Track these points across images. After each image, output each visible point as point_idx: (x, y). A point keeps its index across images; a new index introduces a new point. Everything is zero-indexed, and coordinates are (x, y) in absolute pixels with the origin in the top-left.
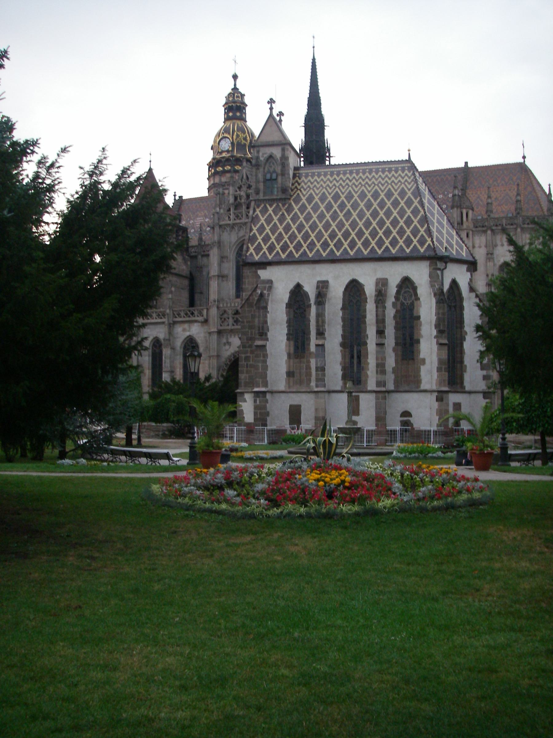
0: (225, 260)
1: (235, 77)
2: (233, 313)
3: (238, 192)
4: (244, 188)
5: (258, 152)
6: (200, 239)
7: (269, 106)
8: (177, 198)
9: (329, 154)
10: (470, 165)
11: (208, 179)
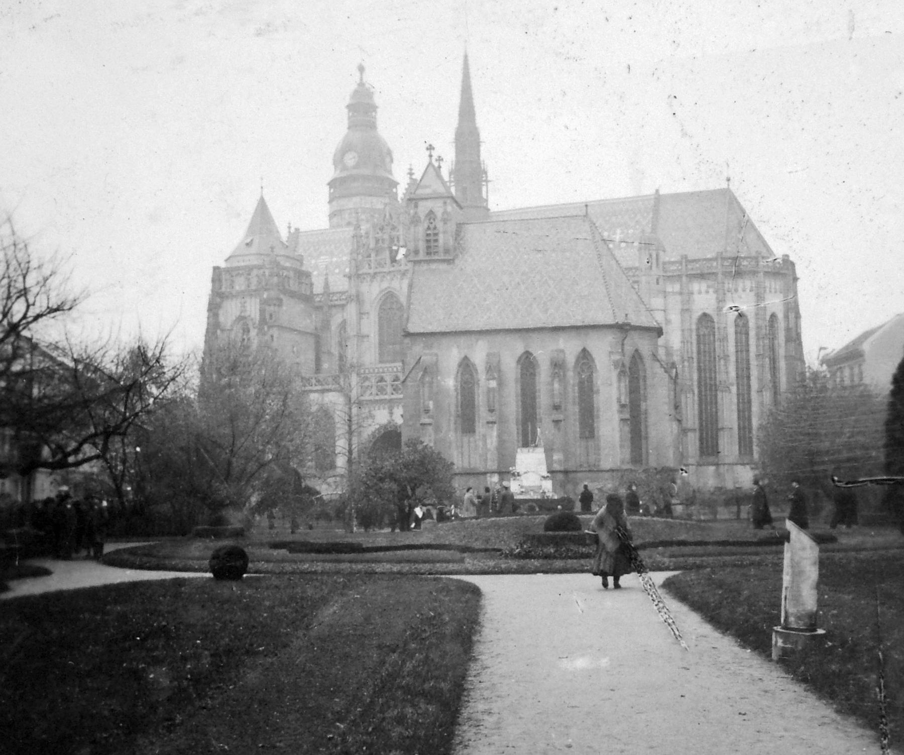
0: (365, 317)
1: (361, 69)
2: (377, 380)
3: (380, 234)
4: (388, 230)
5: (416, 206)
6: (327, 285)
7: (428, 153)
8: (292, 230)
9: (487, 177)
10: (661, 192)
11: (330, 202)
